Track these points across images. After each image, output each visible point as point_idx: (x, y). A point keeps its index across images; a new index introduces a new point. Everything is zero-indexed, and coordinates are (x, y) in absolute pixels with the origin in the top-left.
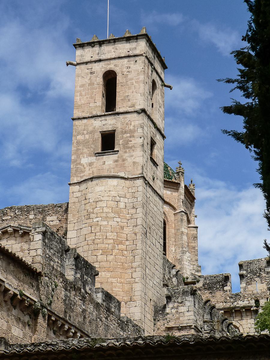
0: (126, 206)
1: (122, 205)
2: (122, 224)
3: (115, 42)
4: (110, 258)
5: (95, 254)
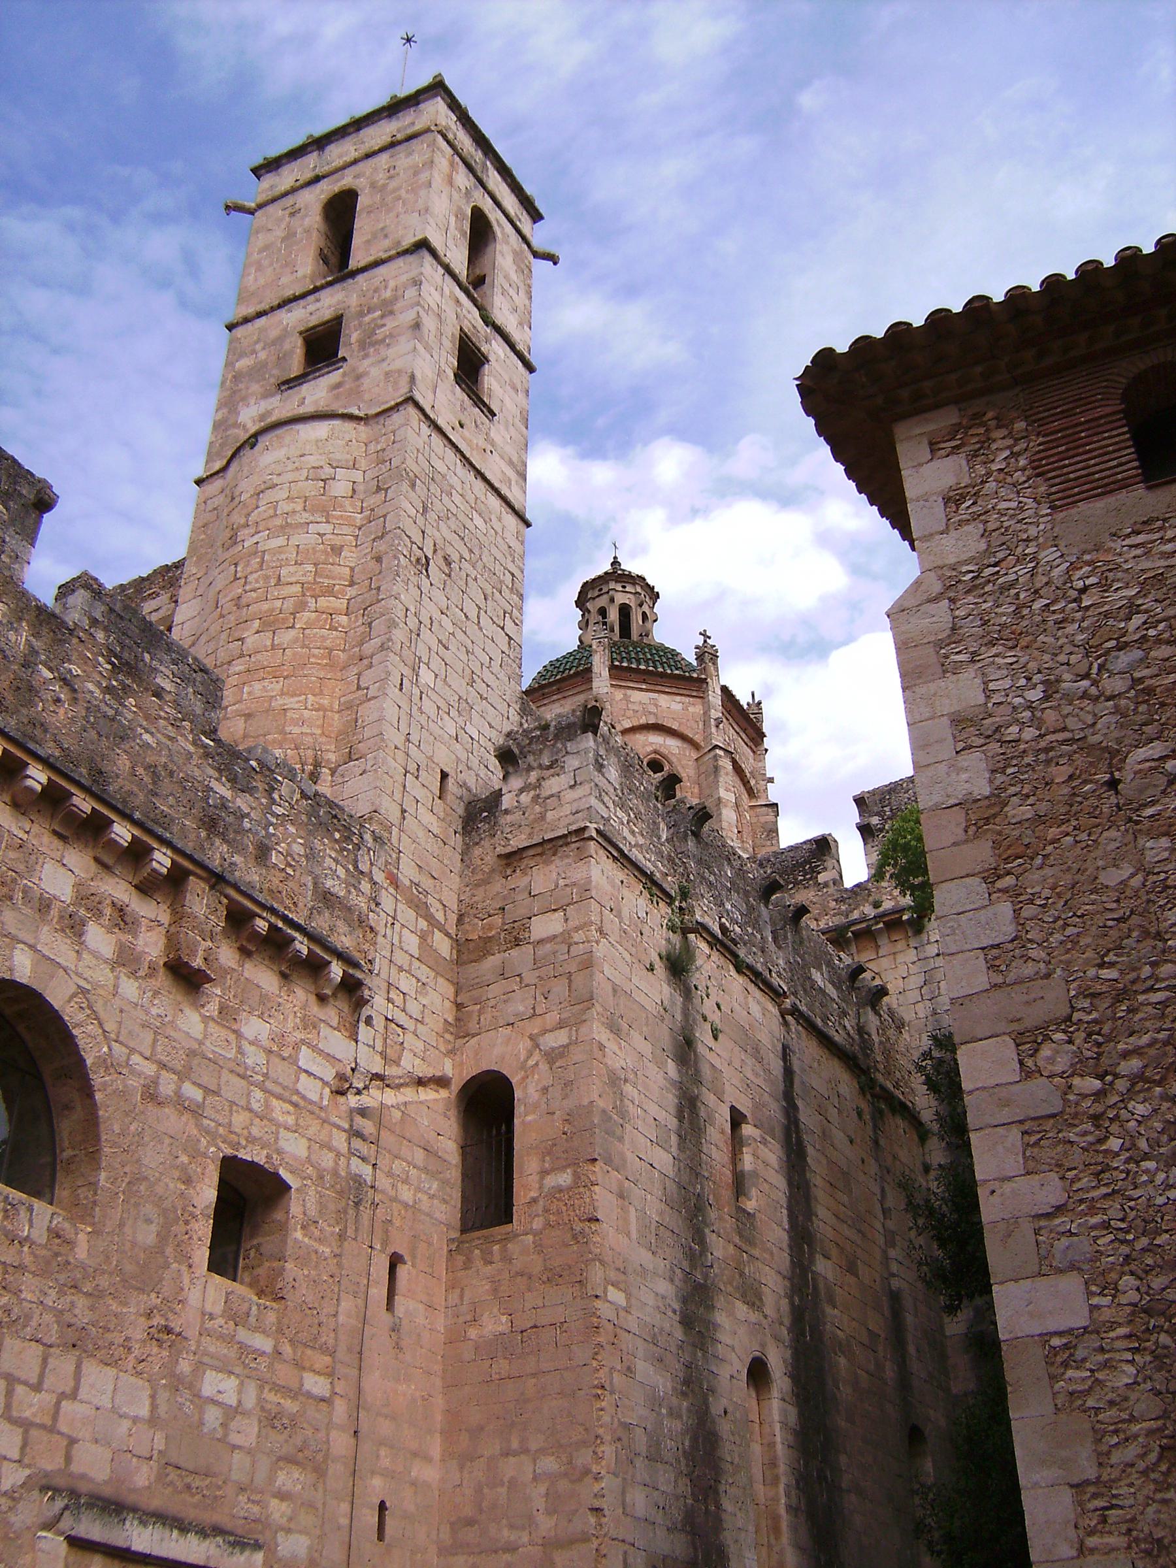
0: (354, 490)
1: (340, 488)
2: (338, 541)
3: (359, 130)
4: (285, 637)
5: (237, 635)
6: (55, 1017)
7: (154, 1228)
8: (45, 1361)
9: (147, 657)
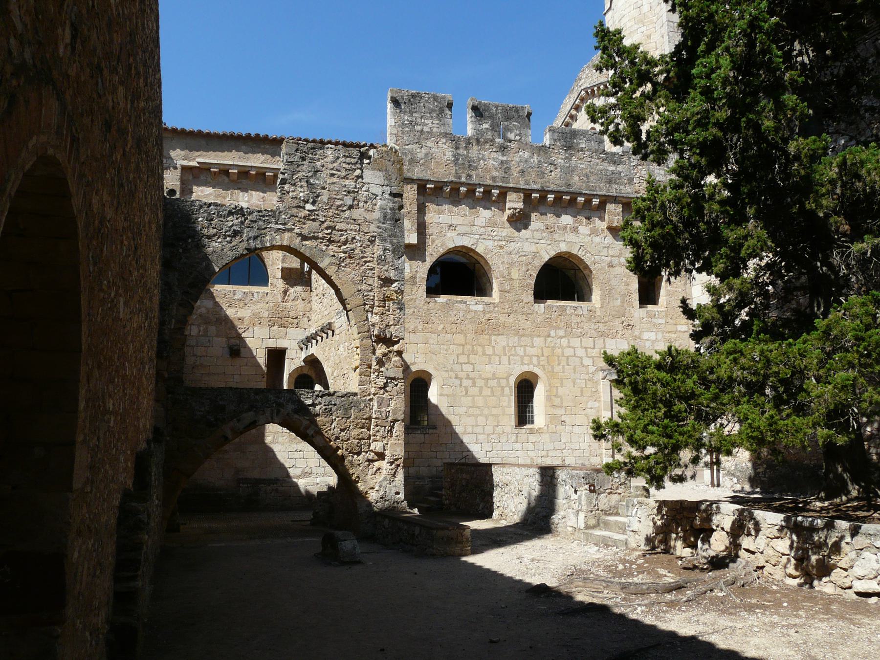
2: (648, 33)
6: (576, 256)
7: (619, 301)
8: (594, 342)
9: (575, 141)
